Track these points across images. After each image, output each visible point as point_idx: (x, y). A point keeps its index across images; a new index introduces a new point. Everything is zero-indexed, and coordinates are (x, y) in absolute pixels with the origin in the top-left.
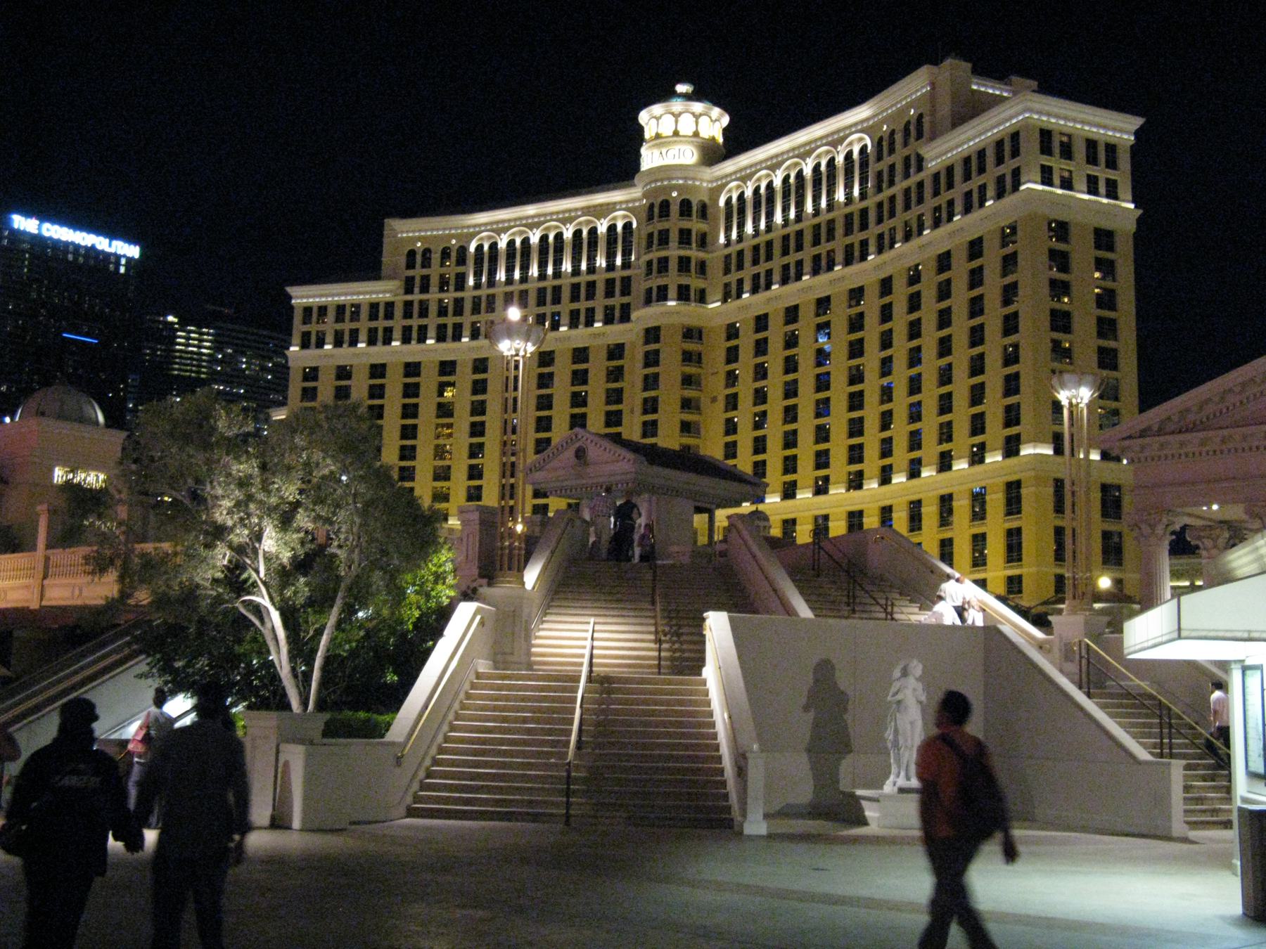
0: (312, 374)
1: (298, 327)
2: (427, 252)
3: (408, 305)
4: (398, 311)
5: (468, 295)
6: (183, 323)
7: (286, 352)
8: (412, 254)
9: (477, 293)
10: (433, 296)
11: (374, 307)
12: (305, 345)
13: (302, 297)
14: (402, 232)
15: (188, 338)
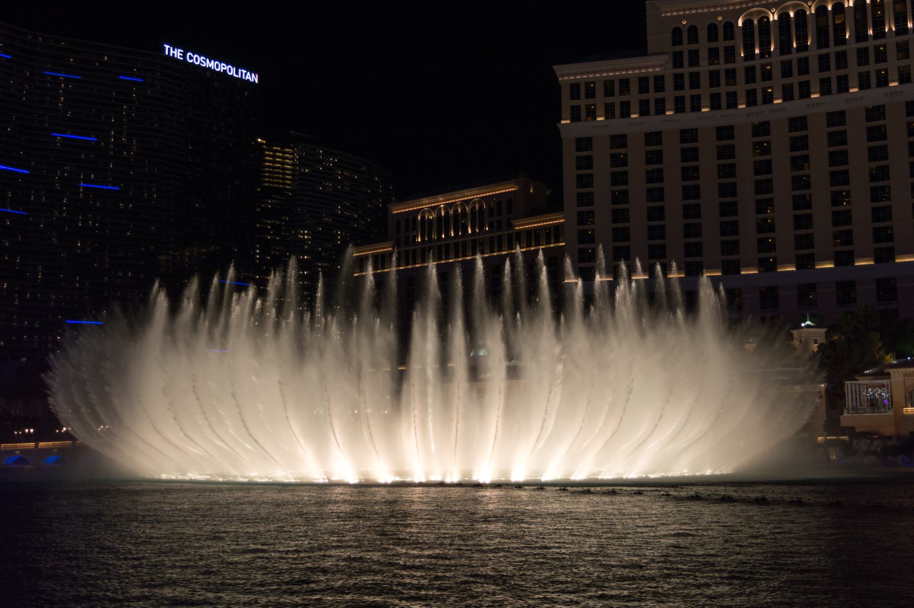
0: (584, 143)
1: (567, 102)
2: (693, 30)
3: (678, 79)
4: (669, 83)
5: (740, 65)
6: (270, 145)
7: (558, 125)
8: (677, 32)
9: (750, 63)
10: (704, 67)
11: (643, 81)
12: (575, 118)
13: (569, 75)
14: (666, 12)
15: (274, 157)
